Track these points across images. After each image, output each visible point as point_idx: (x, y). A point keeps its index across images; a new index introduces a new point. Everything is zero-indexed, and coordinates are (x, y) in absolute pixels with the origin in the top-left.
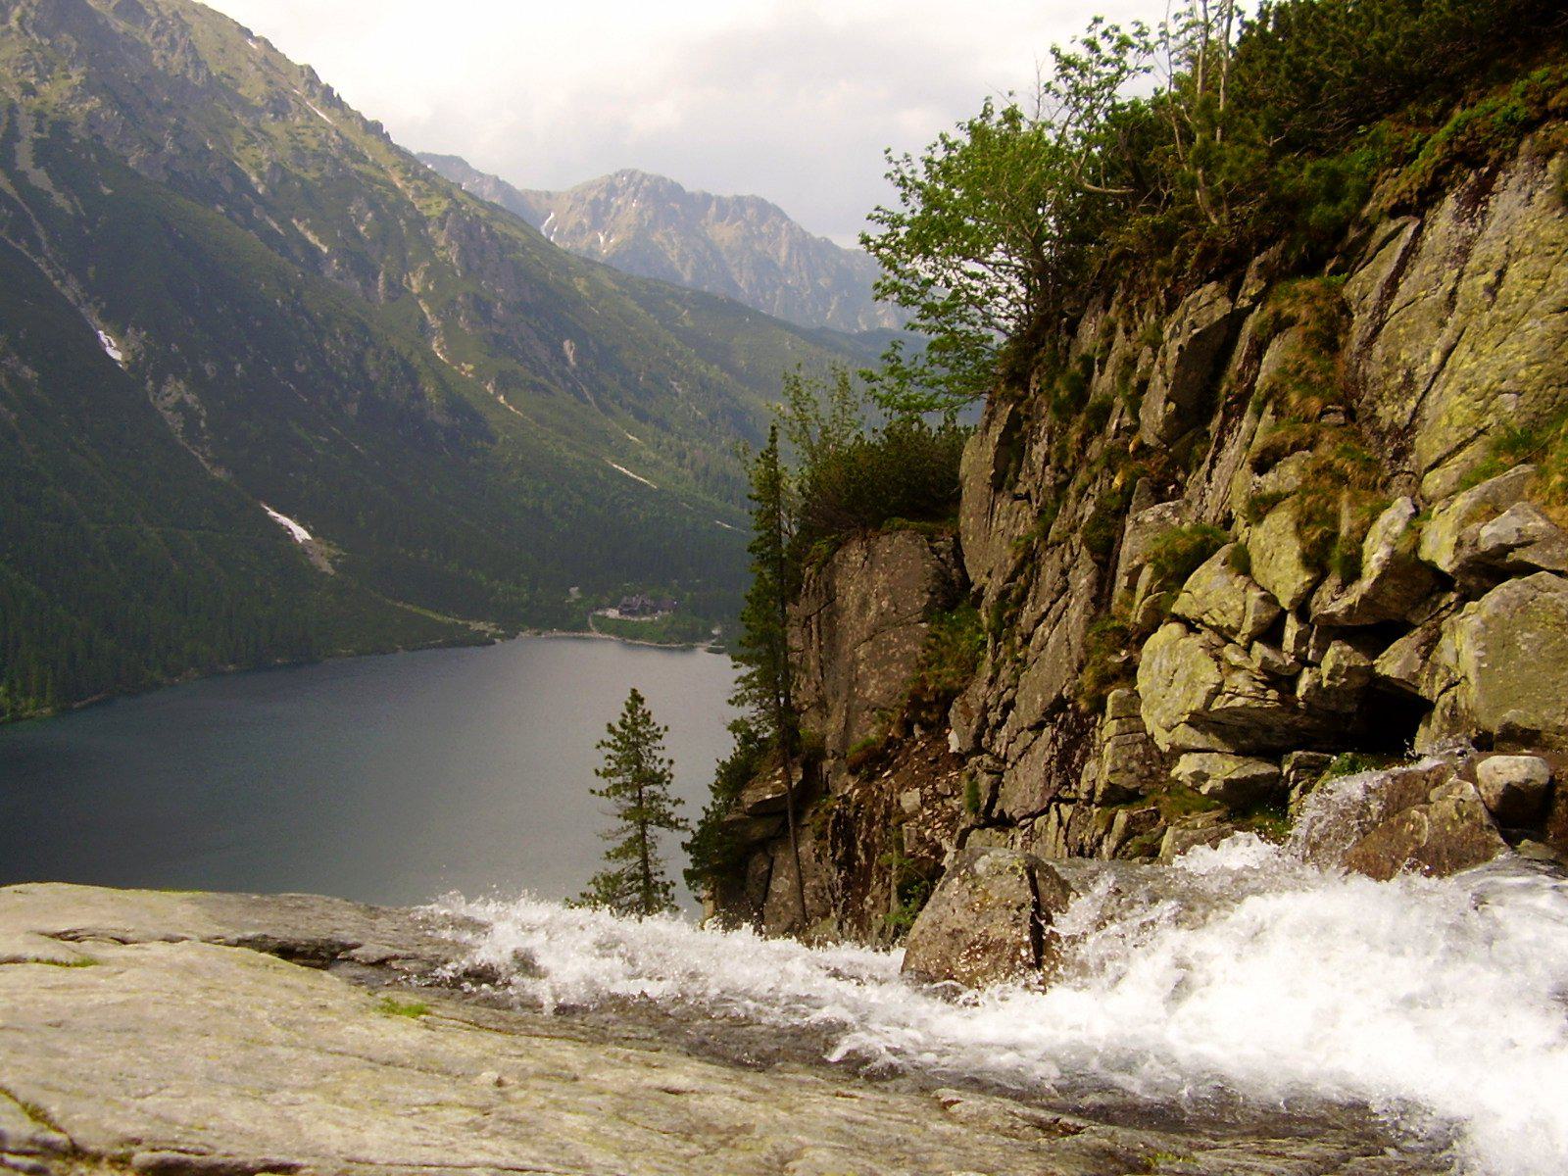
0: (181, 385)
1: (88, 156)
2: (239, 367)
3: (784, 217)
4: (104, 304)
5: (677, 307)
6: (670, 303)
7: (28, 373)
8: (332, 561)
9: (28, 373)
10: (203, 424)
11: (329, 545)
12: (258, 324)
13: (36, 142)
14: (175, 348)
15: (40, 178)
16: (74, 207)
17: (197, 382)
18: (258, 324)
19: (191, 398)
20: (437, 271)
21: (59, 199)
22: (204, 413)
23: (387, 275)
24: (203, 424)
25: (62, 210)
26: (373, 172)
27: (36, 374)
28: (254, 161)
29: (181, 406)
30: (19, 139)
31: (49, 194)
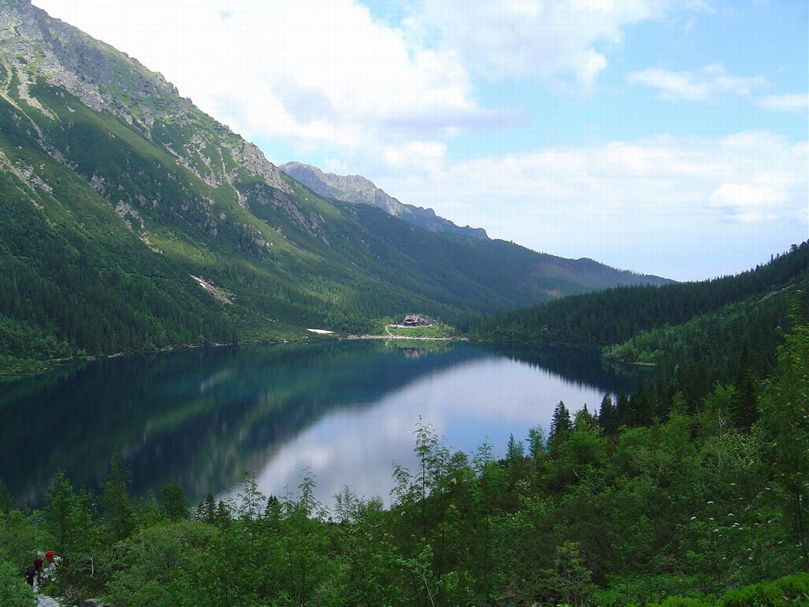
0: (127, 205)
1: (59, 94)
2: (155, 202)
4: (77, 165)
5: (351, 210)
7: (48, 188)
8: (229, 298)
9: (48, 188)
11: (225, 291)
13: (30, 86)
15: (34, 103)
16: (55, 117)
17: (136, 205)
19: (134, 213)
21: (45, 112)
23: (216, 173)
27: (51, 189)
29: (128, 217)
30: (20, 84)
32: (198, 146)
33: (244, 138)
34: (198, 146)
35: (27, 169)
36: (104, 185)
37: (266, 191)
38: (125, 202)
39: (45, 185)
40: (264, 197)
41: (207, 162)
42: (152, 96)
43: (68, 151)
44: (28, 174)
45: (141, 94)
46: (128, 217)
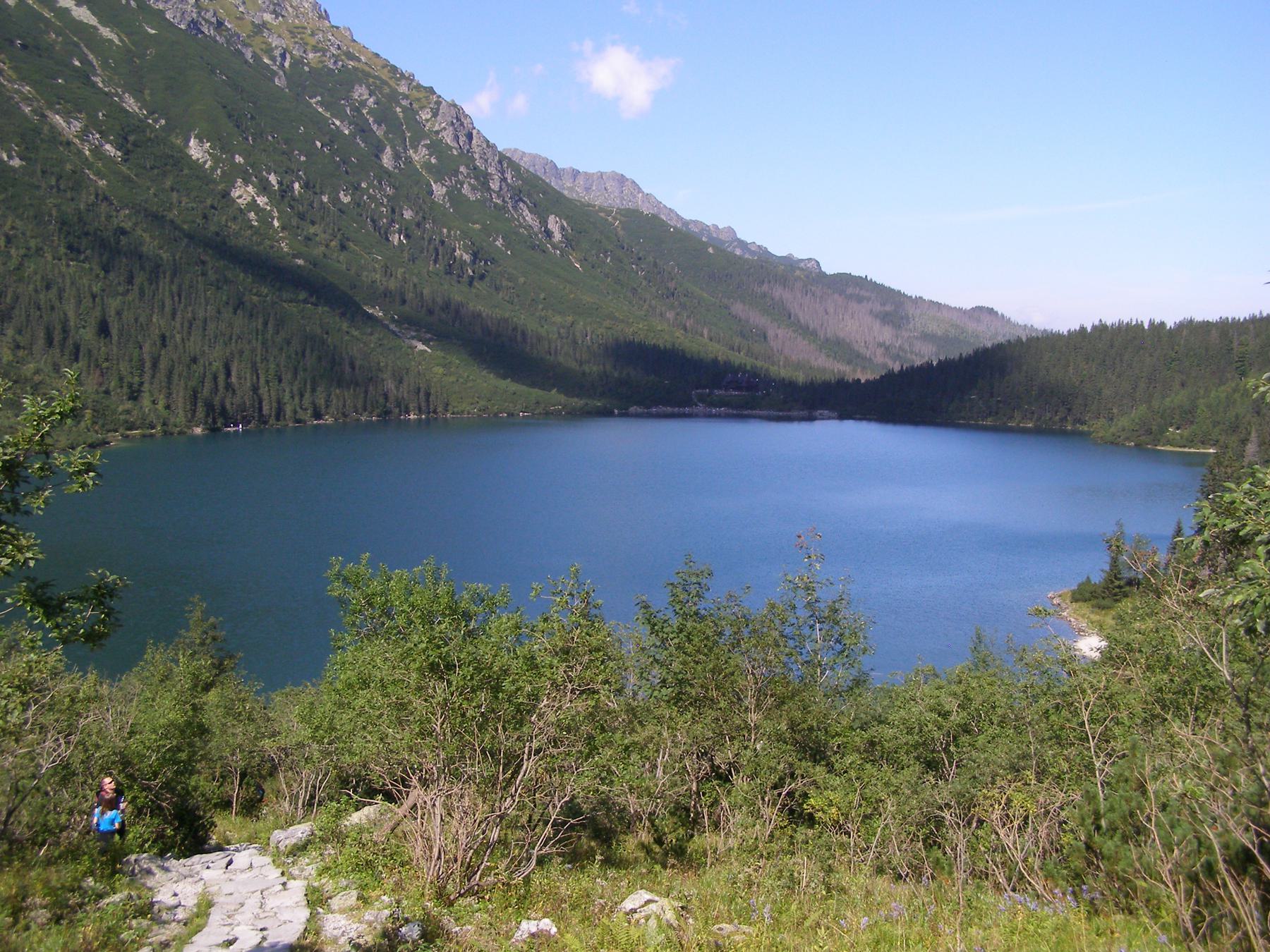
0: (250, 189)
2: (297, 186)
3: (640, 191)
4: (163, 122)
5: (610, 219)
6: (602, 214)
10: (276, 224)
12: (303, 158)
14: (239, 159)
16: (121, 40)
17: (264, 188)
18: (303, 158)
19: (262, 201)
20: (436, 147)
21: (106, 32)
22: (276, 214)
23: (393, 148)
24: (276, 224)
25: (111, 41)
26: (367, 69)
28: (264, 46)
29: (253, 205)
31: (95, 28)
32: (363, 103)
33: (438, 92)
34: (363, 103)
35: (76, 119)
36: (210, 154)
37: (477, 178)
38: (246, 182)
39: (108, 147)
40: (473, 188)
41: (379, 132)
42: (286, 22)
43: (148, 98)
44: (77, 126)
45: (268, 17)
46: (253, 205)
